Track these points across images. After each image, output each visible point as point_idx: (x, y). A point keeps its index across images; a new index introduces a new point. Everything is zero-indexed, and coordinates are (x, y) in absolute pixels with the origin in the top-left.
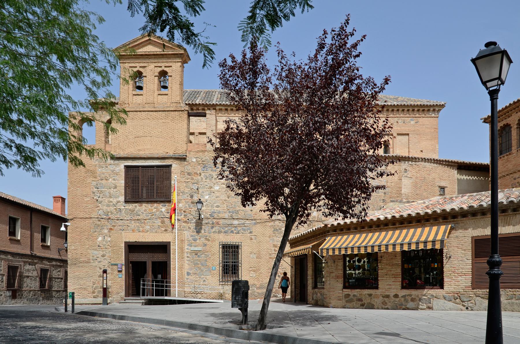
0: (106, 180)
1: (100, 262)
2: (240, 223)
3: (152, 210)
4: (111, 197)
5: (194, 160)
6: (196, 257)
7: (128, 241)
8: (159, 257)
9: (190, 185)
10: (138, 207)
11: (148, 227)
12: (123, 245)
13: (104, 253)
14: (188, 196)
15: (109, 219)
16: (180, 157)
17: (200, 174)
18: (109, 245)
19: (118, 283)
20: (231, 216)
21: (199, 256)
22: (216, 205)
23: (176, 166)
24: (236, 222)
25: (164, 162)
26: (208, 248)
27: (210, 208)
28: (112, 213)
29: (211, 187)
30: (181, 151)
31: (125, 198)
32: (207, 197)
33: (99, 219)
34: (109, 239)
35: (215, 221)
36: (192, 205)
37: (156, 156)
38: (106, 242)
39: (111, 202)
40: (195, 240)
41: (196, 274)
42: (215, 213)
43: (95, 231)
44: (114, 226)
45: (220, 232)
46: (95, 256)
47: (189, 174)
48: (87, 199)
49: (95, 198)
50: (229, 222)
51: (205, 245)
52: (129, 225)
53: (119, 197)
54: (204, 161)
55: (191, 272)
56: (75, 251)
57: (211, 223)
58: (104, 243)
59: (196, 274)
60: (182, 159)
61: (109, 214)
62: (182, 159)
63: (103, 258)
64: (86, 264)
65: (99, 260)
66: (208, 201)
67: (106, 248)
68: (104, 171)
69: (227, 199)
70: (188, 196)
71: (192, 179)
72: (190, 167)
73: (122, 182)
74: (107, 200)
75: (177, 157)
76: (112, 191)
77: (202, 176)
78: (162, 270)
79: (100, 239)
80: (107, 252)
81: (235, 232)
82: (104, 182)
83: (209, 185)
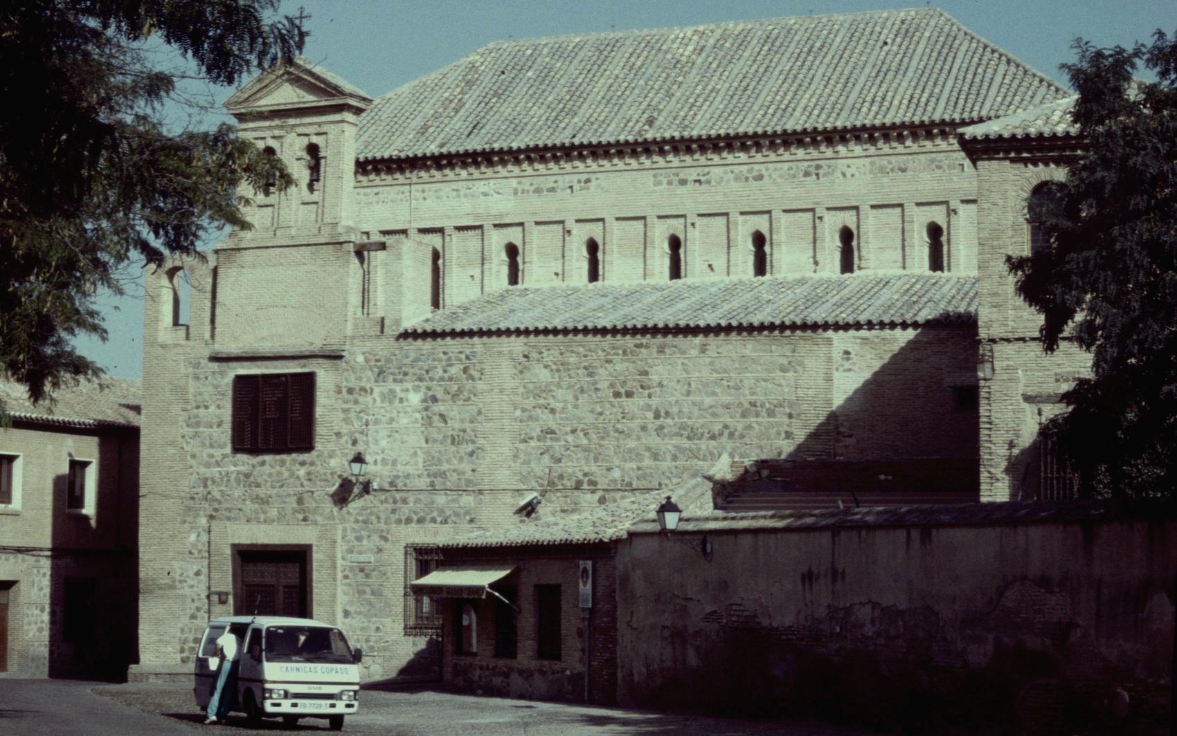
1: (192, 586)
4: (212, 446)
5: (360, 359)
7: (237, 542)
17: (372, 390)
20: (432, 484)
21: (367, 576)
25: (304, 366)
26: (384, 556)
27: (389, 467)
28: (214, 482)
29: (392, 420)
37: (290, 351)
39: (212, 456)
40: (359, 539)
41: (360, 613)
43: (185, 522)
48: (171, 451)
51: (380, 550)
55: (351, 609)
59: (360, 613)
61: (209, 483)
69: (424, 445)
71: (356, 402)
79: (193, 537)
81: (439, 519)
83: (388, 415)
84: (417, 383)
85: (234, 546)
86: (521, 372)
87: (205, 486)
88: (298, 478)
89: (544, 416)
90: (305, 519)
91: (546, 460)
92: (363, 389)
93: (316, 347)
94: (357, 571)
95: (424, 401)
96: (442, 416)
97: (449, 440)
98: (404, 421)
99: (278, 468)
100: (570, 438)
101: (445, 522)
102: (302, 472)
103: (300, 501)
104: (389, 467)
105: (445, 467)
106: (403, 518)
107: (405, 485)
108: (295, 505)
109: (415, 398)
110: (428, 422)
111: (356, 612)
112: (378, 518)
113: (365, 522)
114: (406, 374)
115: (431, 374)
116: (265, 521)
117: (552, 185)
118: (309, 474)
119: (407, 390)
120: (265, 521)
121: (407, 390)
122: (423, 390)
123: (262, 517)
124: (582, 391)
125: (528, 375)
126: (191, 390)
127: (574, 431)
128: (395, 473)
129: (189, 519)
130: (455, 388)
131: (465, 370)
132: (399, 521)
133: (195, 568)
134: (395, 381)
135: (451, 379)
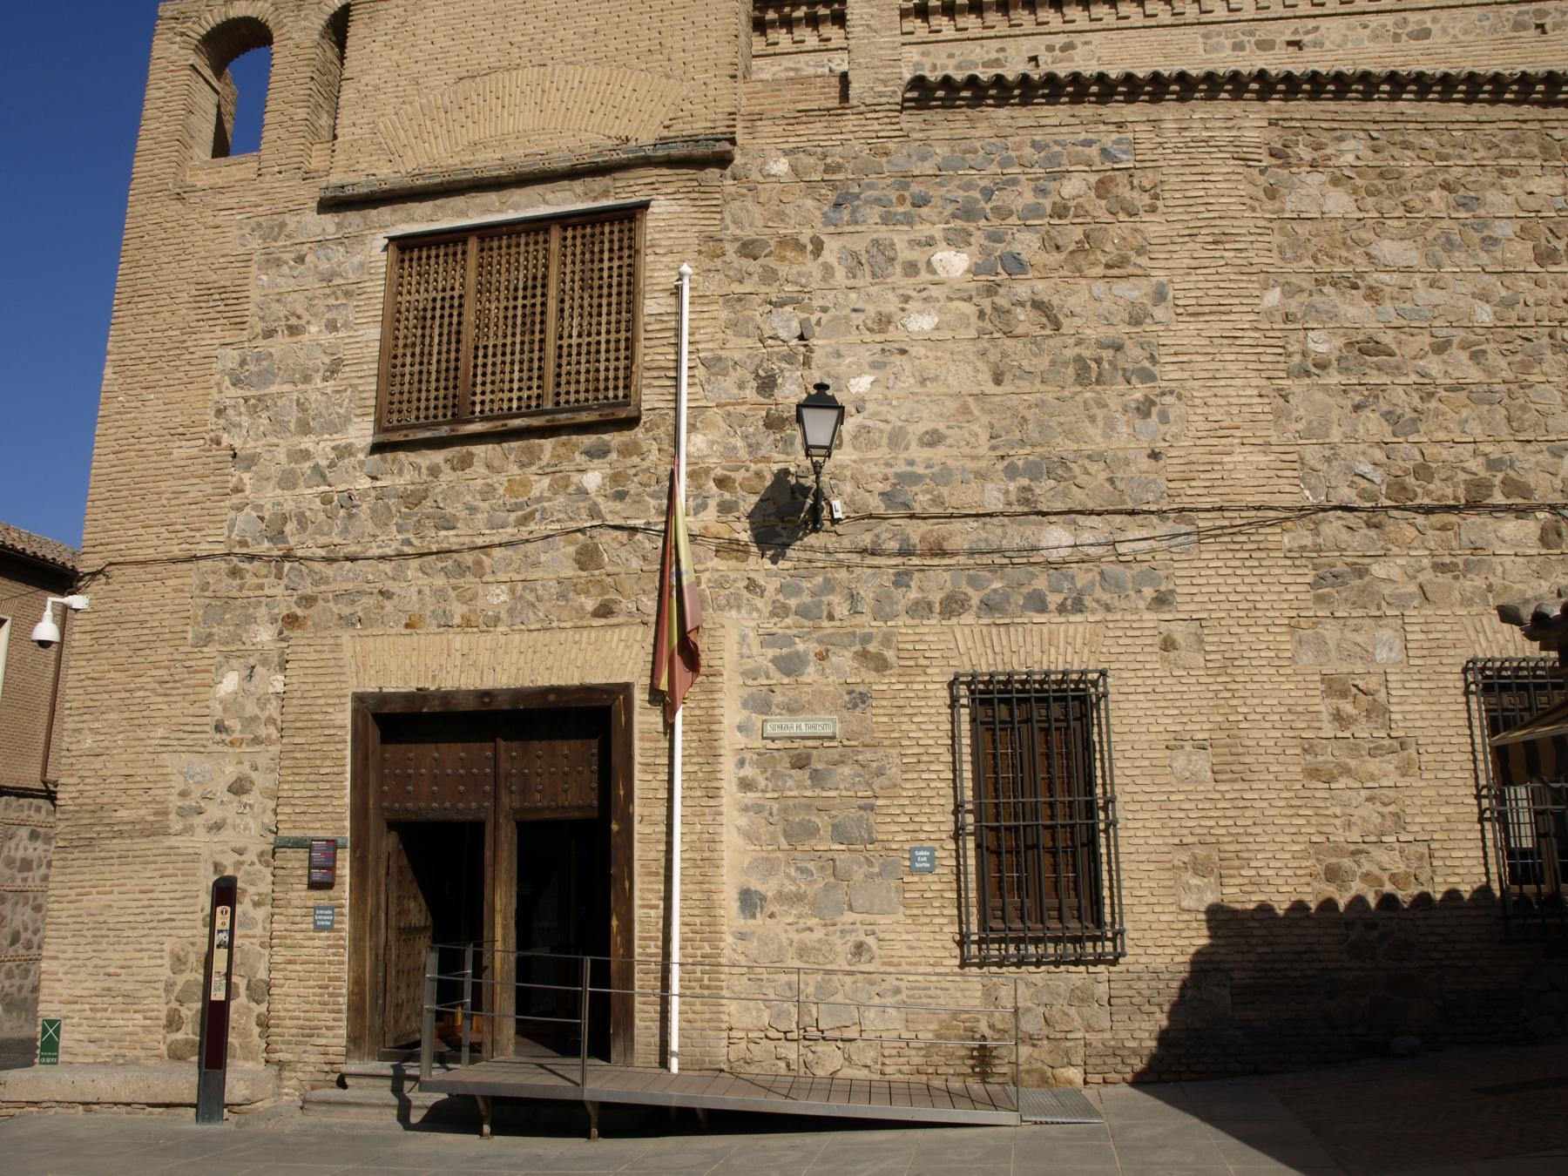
0: (293, 331)
1: (218, 826)
2: (1087, 537)
3: (526, 485)
4: (304, 428)
5: (781, 166)
6: (796, 785)
7: (371, 687)
8: (553, 778)
9: (757, 313)
10: (447, 476)
12: (345, 717)
13: (246, 769)
14: (741, 386)
15: (287, 556)
16: (699, 151)
18: (271, 721)
19: (307, 963)
20: (1026, 495)
21: (817, 778)
22: (921, 428)
23: (669, 212)
24: (1056, 537)
26: (878, 716)
29: (884, 321)
30: (701, 122)
31: (380, 428)
32: (861, 384)
33: (238, 559)
34: (278, 683)
35: (916, 532)
36: (768, 440)
38: (262, 702)
39: (306, 455)
40: (790, 665)
41: (798, 898)
42: (917, 478)
45: (953, 606)
46: (197, 792)
48: (181, 451)
49: (226, 439)
50: (1015, 535)
52: (390, 585)
53: (347, 420)
54: (838, 168)
55: (769, 888)
56: (97, 763)
57: (894, 545)
58: (251, 709)
59: (798, 898)
60: (704, 158)
61: (290, 527)
62: (704, 158)
64: (143, 844)
65: (213, 812)
66: (870, 407)
67: (257, 741)
68: (286, 284)
69: (990, 388)
70: (741, 386)
71: (770, 276)
72: (757, 211)
75: (678, 151)
76: (318, 391)
77: (828, 256)
78: (580, 872)
79: (230, 682)
80: (263, 761)
81: (1054, 600)
82: (279, 345)
83: (871, 310)
84: (959, 223)
85: (359, 699)
86: (1272, 193)
87: (279, 536)
88: (582, 492)
89: (1355, 310)
90: (604, 611)
91: (1373, 425)
93: (645, 136)
94: (784, 766)
95: (975, 270)
96: (1038, 305)
97: (1071, 371)
98: (922, 322)
99: (514, 469)
100: (1433, 365)
101: (1078, 606)
102: (593, 479)
103: (587, 558)
104: (883, 452)
106: (936, 597)
107: (937, 500)
108: (570, 571)
109: (954, 263)
110: (999, 321)
111: (782, 897)
112: (853, 597)
113: (803, 612)
114: (921, 202)
115: (998, 199)
116: (467, 623)
117: (994, 55)
118: (616, 478)
120: (467, 623)
121: (930, 242)
122: (978, 238)
123: (458, 610)
124: (1449, 245)
125: (1291, 204)
126: (255, 295)
127: (1440, 348)
128: (902, 468)
130: (1078, 233)
131: (1102, 189)
132: (920, 609)
133: (231, 771)
134: (886, 220)
135: (1060, 211)
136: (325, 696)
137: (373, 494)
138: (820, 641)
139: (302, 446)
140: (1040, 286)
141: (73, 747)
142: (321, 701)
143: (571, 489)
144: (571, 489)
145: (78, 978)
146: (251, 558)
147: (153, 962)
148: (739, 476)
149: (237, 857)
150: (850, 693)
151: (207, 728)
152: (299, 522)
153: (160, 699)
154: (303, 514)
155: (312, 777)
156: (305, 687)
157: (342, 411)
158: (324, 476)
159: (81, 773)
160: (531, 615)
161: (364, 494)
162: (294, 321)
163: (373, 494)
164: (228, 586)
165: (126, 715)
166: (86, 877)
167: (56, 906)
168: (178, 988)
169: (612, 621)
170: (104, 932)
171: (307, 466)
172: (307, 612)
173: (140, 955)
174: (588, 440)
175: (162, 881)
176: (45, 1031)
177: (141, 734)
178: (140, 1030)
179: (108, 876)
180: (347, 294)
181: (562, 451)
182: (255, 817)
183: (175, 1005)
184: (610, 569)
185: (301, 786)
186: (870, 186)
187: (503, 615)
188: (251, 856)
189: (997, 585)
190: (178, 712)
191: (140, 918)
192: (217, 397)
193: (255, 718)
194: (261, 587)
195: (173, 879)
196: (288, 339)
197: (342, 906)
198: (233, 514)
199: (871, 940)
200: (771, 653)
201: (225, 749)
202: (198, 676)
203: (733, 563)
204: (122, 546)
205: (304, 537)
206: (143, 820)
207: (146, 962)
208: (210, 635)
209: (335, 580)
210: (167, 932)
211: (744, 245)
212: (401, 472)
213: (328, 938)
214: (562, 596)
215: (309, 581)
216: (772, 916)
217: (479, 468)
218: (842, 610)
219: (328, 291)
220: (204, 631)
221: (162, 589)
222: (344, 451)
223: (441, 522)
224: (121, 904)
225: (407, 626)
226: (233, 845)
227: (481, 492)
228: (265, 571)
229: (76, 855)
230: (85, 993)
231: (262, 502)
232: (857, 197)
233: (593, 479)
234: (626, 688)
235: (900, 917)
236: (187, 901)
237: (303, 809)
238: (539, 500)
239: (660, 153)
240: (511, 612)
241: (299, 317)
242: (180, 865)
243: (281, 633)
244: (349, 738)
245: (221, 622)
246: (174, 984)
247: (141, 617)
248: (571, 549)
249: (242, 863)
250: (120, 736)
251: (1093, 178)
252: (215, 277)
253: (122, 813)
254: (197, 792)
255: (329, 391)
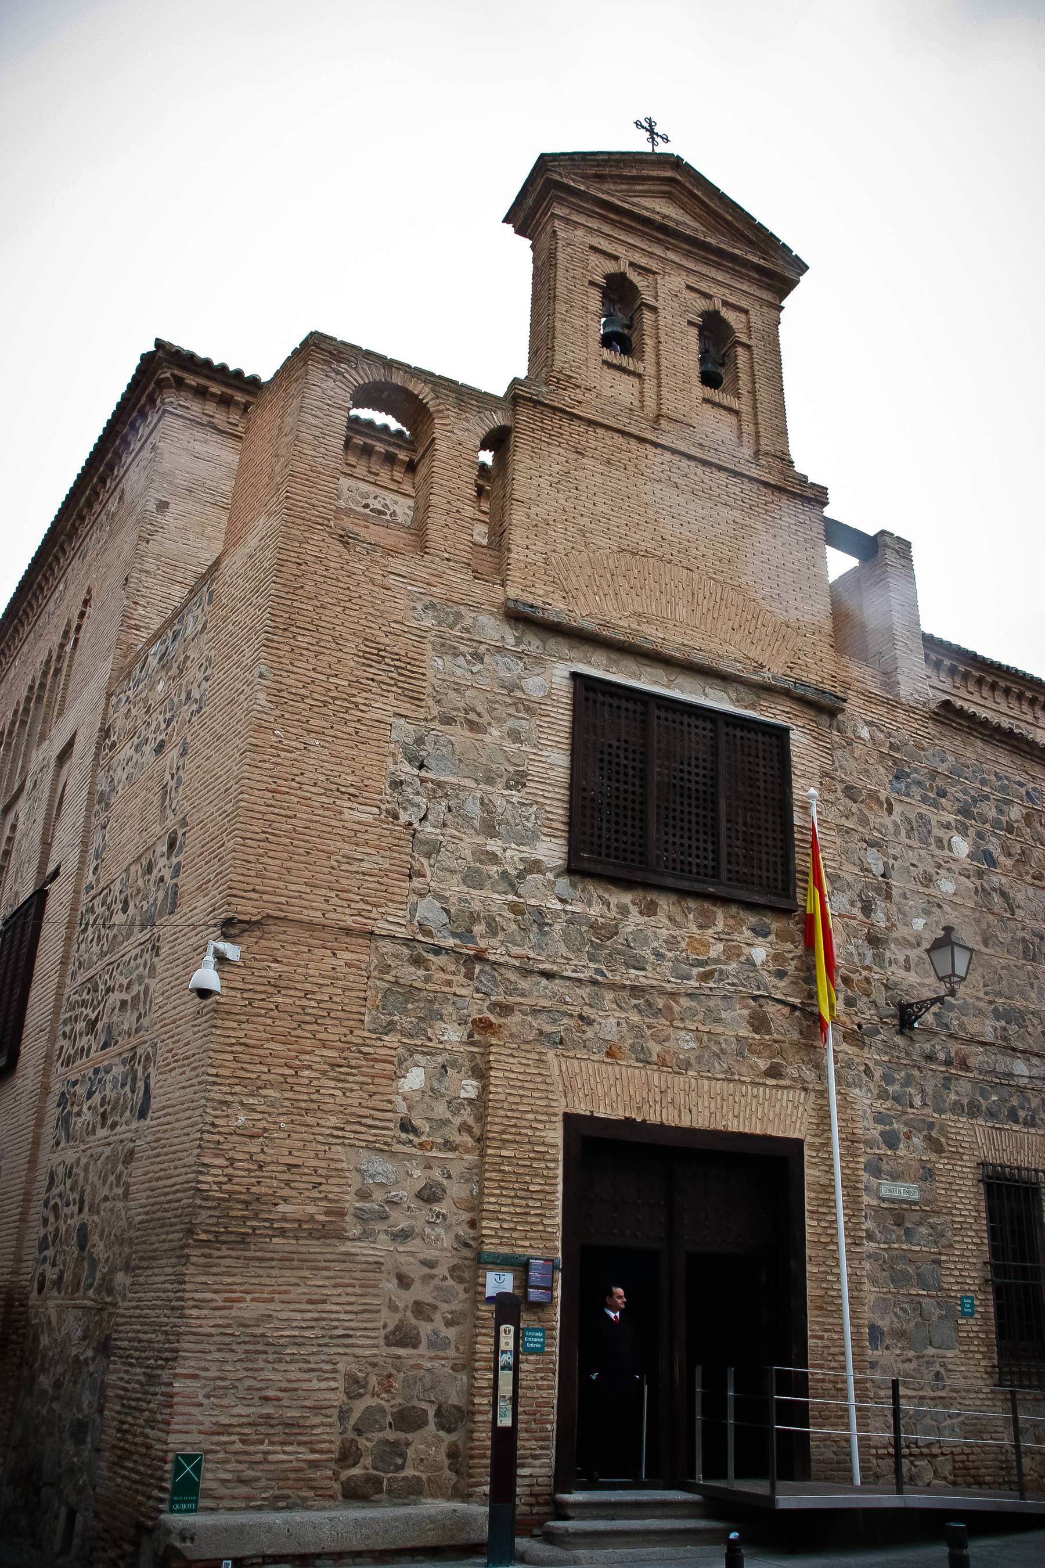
0: (473, 726)
1: (404, 1235)
3: (707, 946)
4: (489, 829)
10: (636, 918)
11: (685, 1043)
13: (437, 1174)
18: (465, 1128)
25: (752, 706)
28: (493, 928)
33: (419, 950)
35: (954, 1047)
39: (493, 858)
40: (891, 1140)
43: (390, 1027)
44: (505, 1010)
46: (379, 1195)
47: (850, 792)
48: (356, 814)
52: (587, 1011)
55: (884, 1324)
56: (254, 1147)
57: (942, 1056)
58: (441, 1110)
61: (479, 929)
63: (423, 1213)
64: (314, 1247)
67: (448, 1145)
71: (864, 821)
73: (553, 760)
74: (469, 842)
76: (499, 796)
77: (896, 816)
79: (415, 1079)
80: (456, 1169)
87: (466, 935)
88: (750, 962)
90: (774, 1072)
92: (873, 796)
96: (1003, 894)
99: (694, 929)
102: (760, 953)
105: (1020, 1003)
108: (745, 1032)
109: (962, 847)
114: (942, 794)
119: (948, 826)
121: (948, 826)
129: (406, 1022)
136: (532, 1112)
137: (564, 917)
138: (906, 1124)
139: (489, 848)
140: (1004, 880)
141: (220, 1122)
142: (530, 1116)
143: (743, 959)
144: (743, 959)
145: (224, 1402)
146: (438, 950)
147: (324, 1385)
148: (855, 977)
149: (427, 1271)
150: (923, 1168)
151: (391, 1125)
152: (489, 925)
153: (332, 1084)
154: (494, 919)
155: (520, 1193)
156: (511, 1099)
157: (530, 825)
158: (512, 885)
159: (231, 1154)
160: (716, 1065)
161: (556, 914)
162: (472, 716)
163: (564, 917)
164: (413, 975)
165: (290, 1095)
166: (238, 1279)
167: (194, 1312)
168: (356, 1415)
169: (782, 1082)
170: (260, 1347)
171: (494, 869)
172: (503, 1020)
173: (307, 1376)
174: (753, 919)
175: (335, 1291)
176: (178, 1468)
177: (310, 1120)
178: (304, 1465)
179: (267, 1281)
180: (528, 709)
181: (732, 922)
182: (448, 1228)
183: (351, 1435)
184: (776, 1036)
185: (509, 1201)
186: (916, 771)
187: (693, 1062)
188: (442, 1271)
189: (994, 1098)
190: (356, 1102)
191: (308, 1333)
192: (392, 768)
193: (445, 1123)
194: (449, 983)
195: (349, 1290)
196: (468, 734)
197: (554, 1329)
198: (413, 898)
199: (942, 1371)
200: (880, 1127)
201: (414, 1151)
202: (378, 1065)
203: (855, 1049)
204: (283, 900)
205: (494, 942)
206: (312, 1219)
207: (315, 1384)
208: (392, 1023)
209: (531, 993)
210: (341, 1350)
211: (847, 787)
212: (589, 904)
213: (537, 1362)
214: (740, 1054)
215: (501, 990)
216: (887, 1348)
217: (661, 918)
218: (917, 1101)
219: (509, 700)
220: (385, 1019)
221: (333, 961)
222: (534, 866)
223: (632, 962)
224: (285, 1315)
225: (609, 1054)
226: (422, 1256)
227: (666, 942)
228: (453, 968)
229: (225, 1252)
230: (234, 1421)
231: (447, 894)
232: (908, 775)
233: (760, 953)
234: (799, 1143)
235: (957, 1352)
236: (367, 1316)
237: (511, 1225)
238: (717, 961)
239: (799, 691)
240: (699, 1059)
241: (479, 715)
242: (358, 1275)
243: (470, 1035)
244: (561, 1157)
245: (404, 1011)
246: (350, 1410)
247: (308, 986)
248: (745, 1012)
249: (432, 1277)
250: (282, 1118)
251: (1024, 811)
252: (386, 641)
253: (283, 1208)
254: (379, 1195)
255: (515, 800)
